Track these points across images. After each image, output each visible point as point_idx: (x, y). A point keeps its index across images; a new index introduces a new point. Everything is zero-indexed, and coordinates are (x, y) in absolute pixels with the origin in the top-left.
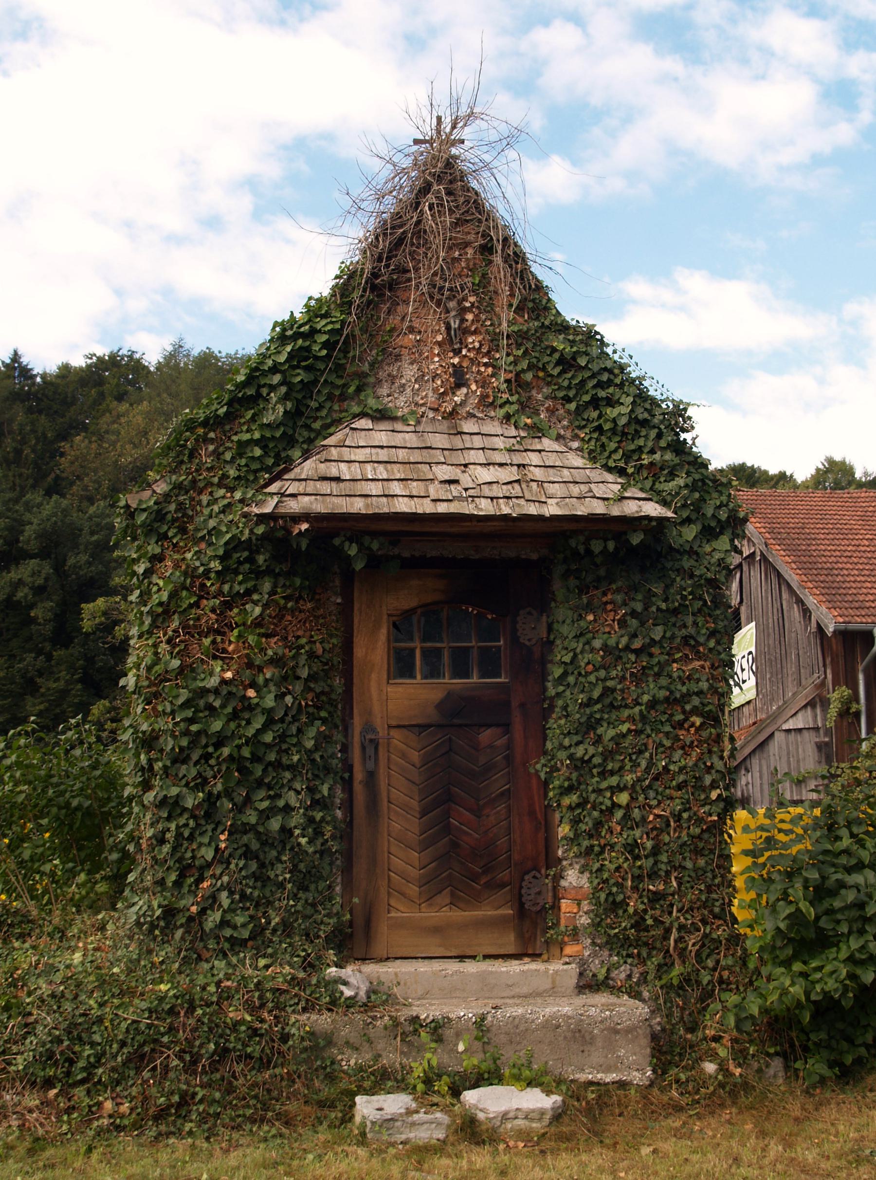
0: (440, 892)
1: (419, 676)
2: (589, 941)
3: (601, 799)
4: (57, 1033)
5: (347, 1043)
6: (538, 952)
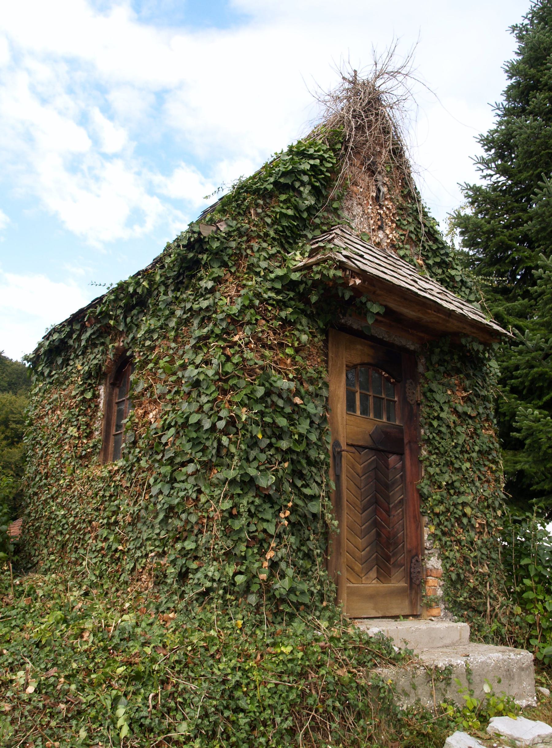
0: (371, 569)
1: (358, 413)
2: (443, 606)
3: (455, 510)
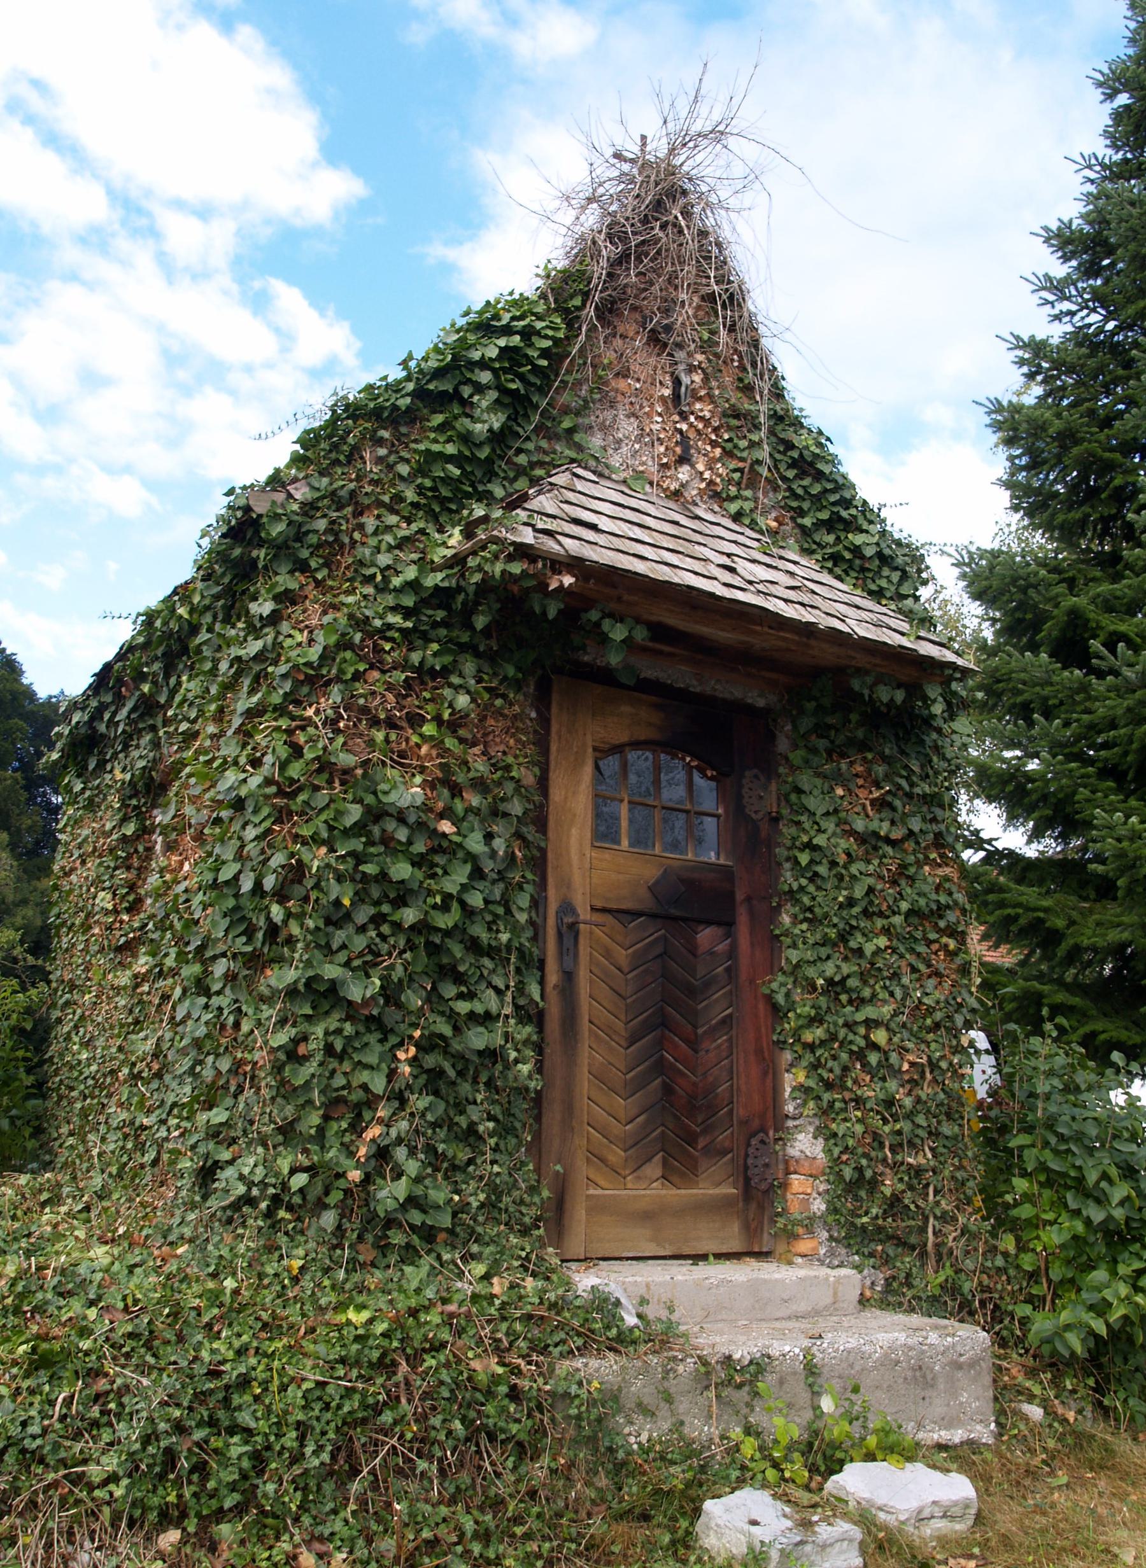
0: (649, 1160)
1: (625, 843)
2: (826, 1235)
3: (851, 1037)
4: (177, 1413)
5: (639, 1405)
6: (765, 1250)
